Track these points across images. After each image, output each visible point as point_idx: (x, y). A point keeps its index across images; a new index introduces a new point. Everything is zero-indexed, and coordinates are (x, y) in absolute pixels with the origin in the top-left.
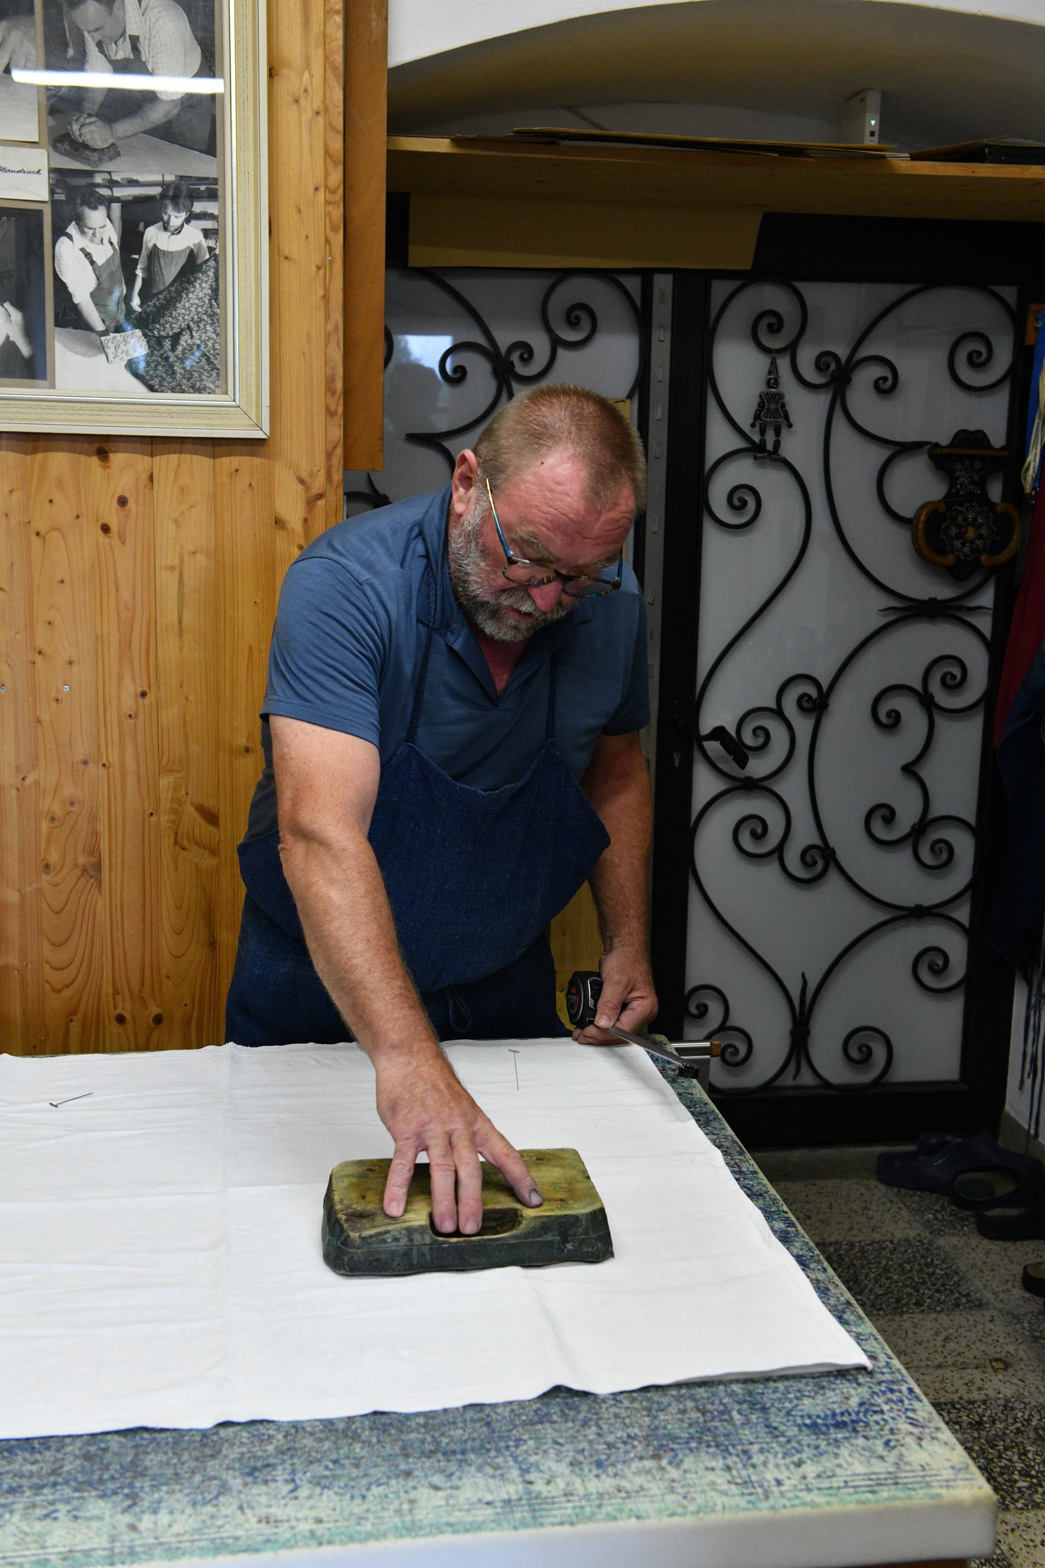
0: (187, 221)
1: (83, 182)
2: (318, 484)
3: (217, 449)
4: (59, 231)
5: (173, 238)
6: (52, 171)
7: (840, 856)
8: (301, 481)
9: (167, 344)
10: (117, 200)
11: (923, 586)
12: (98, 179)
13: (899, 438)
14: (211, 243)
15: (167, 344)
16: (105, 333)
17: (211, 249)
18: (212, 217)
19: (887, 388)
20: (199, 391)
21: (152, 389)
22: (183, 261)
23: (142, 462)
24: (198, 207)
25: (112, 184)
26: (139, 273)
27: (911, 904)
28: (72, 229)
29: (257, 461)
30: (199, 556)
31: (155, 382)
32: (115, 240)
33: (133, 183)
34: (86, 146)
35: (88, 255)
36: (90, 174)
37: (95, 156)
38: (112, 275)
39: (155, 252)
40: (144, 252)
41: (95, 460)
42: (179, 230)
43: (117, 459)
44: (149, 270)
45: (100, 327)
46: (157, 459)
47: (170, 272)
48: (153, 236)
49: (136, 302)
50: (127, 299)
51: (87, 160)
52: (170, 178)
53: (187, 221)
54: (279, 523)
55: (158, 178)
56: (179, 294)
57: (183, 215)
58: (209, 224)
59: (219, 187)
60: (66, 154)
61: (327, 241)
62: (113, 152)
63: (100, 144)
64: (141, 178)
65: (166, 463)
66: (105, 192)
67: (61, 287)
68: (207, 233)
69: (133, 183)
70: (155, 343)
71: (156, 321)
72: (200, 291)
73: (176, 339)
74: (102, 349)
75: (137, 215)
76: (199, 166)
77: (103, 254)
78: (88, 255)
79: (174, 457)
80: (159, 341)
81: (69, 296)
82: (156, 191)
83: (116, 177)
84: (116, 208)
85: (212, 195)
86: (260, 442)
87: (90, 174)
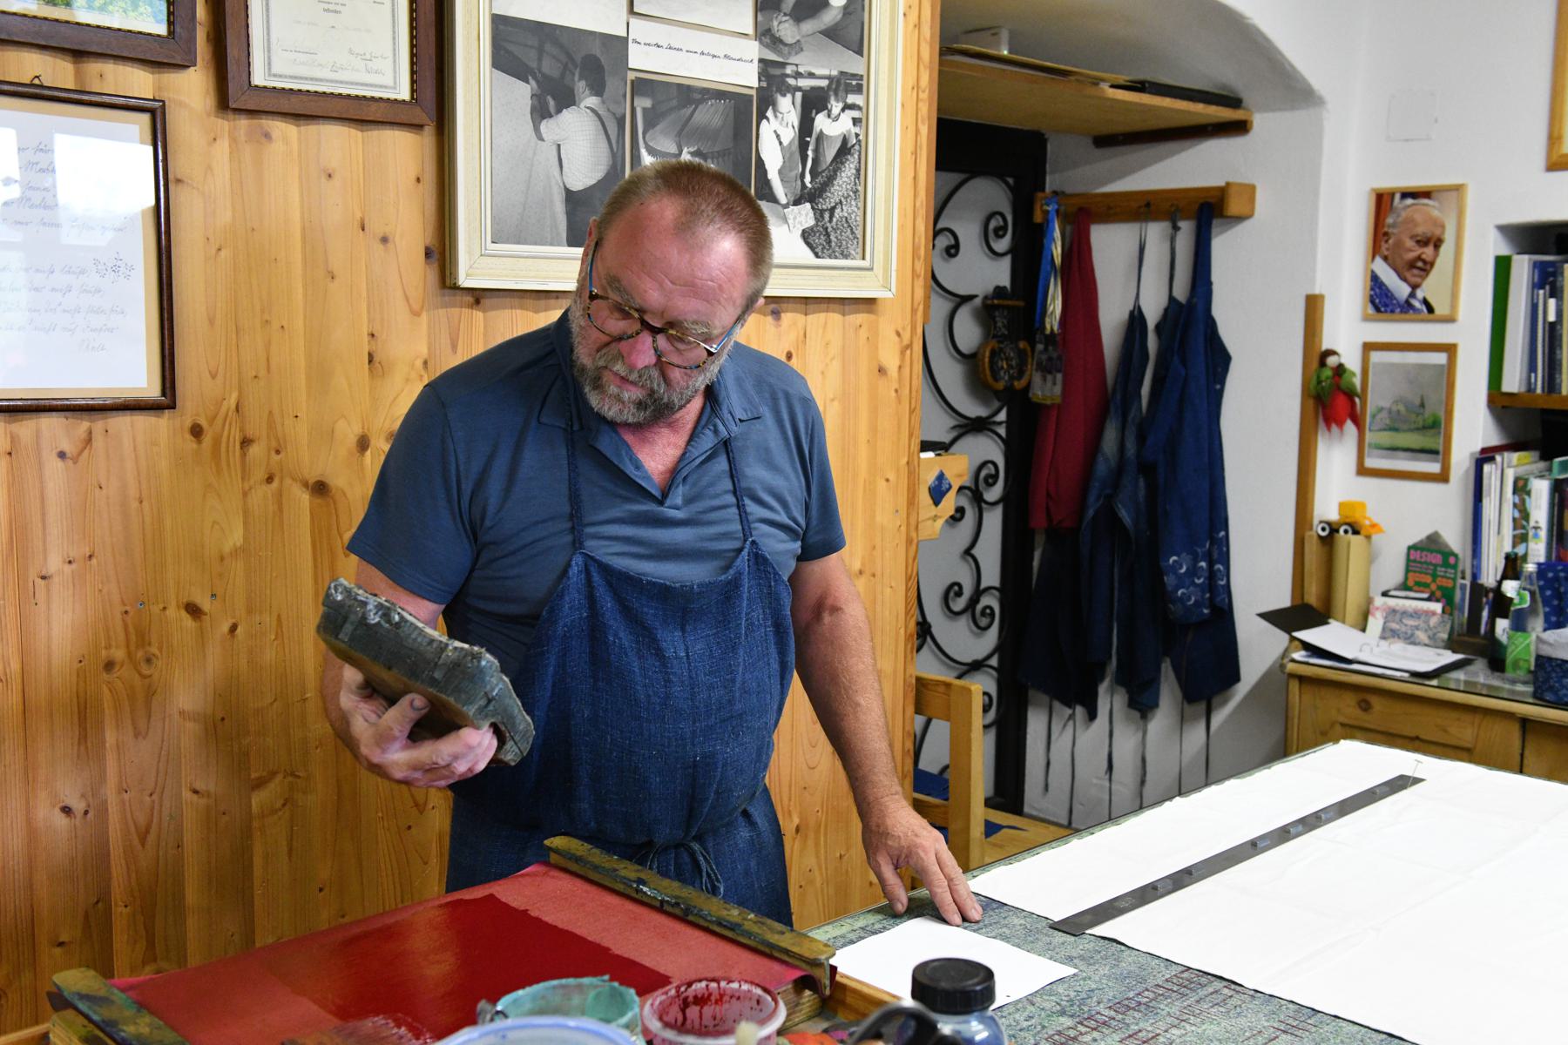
0: (843, 110)
1: (777, 72)
2: (906, 336)
3: (847, 308)
4: (762, 116)
5: (833, 125)
6: (761, 61)
7: (934, 630)
8: (898, 334)
9: (827, 216)
10: (799, 89)
11: (973, 409)
12: (789, 70)
13: (962, 292)
14: (857, 130)
15: (827, 216)
16: (786, 206)
17: (857, 135)
18: (859, 108)
19: (952, 251)
20: (846, 257)
21: (817, 256)
22: (838, 145)
23: (800, 318)
24: (851, 99)
25: (798, 75)
26: (810, 153)
27: (969, 660)
28: (770, 113)
29: (872, 317)
30: (836, 403)
31: (819, 250)
32: (796, 124)
33: (811, 75)
34: (781, 41)
35: (778, 136)
36: (783, 65)
37: (786, 50)
38: (792, 154)
39: (821, 136)
40: (814, 136)
41: (770, 319)
42: (837, 118)
43: (787, 317)
44: (816, 151)
45: (783, 200)
46: (810, 317)
47: (830, 153)
48: (821, 122)
49: (808, 178)
50: (802, 175)
51: (779, 53)
52: (834, 73)
53: (843, 110)
54: (882, 370)
55: (826, 72)
56: (835, 171)
57: (841, 105)
58: (856, 114)
59: (864, 83)
60: (767, 46)
61: (917, 131)
62: (797, 47)
63: (790, 40)
64: (818, 72)
65: (817, 319)
66: (791, 81)
67: (760, 163)
68: (856, 121)
69: (811, 75)
70: (819, 214)
71: (820, 196)
72: (848, 170)
73: (832, 210)
74: (785, 220)
75: (813, 103)
76: (852, 64)
77: (789, 135)
78: (778, 136)
79: (823, 315)
80: (822, 212)
81: (765, 171)
82: (824, 83)
83: (801, 70)
84: (799, 95)
85: (858, 89)
86: (871, 302)
87: (783, 65)
